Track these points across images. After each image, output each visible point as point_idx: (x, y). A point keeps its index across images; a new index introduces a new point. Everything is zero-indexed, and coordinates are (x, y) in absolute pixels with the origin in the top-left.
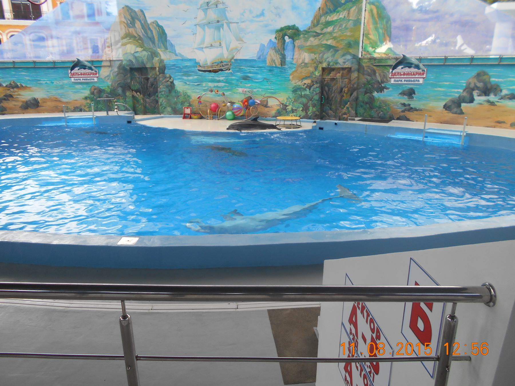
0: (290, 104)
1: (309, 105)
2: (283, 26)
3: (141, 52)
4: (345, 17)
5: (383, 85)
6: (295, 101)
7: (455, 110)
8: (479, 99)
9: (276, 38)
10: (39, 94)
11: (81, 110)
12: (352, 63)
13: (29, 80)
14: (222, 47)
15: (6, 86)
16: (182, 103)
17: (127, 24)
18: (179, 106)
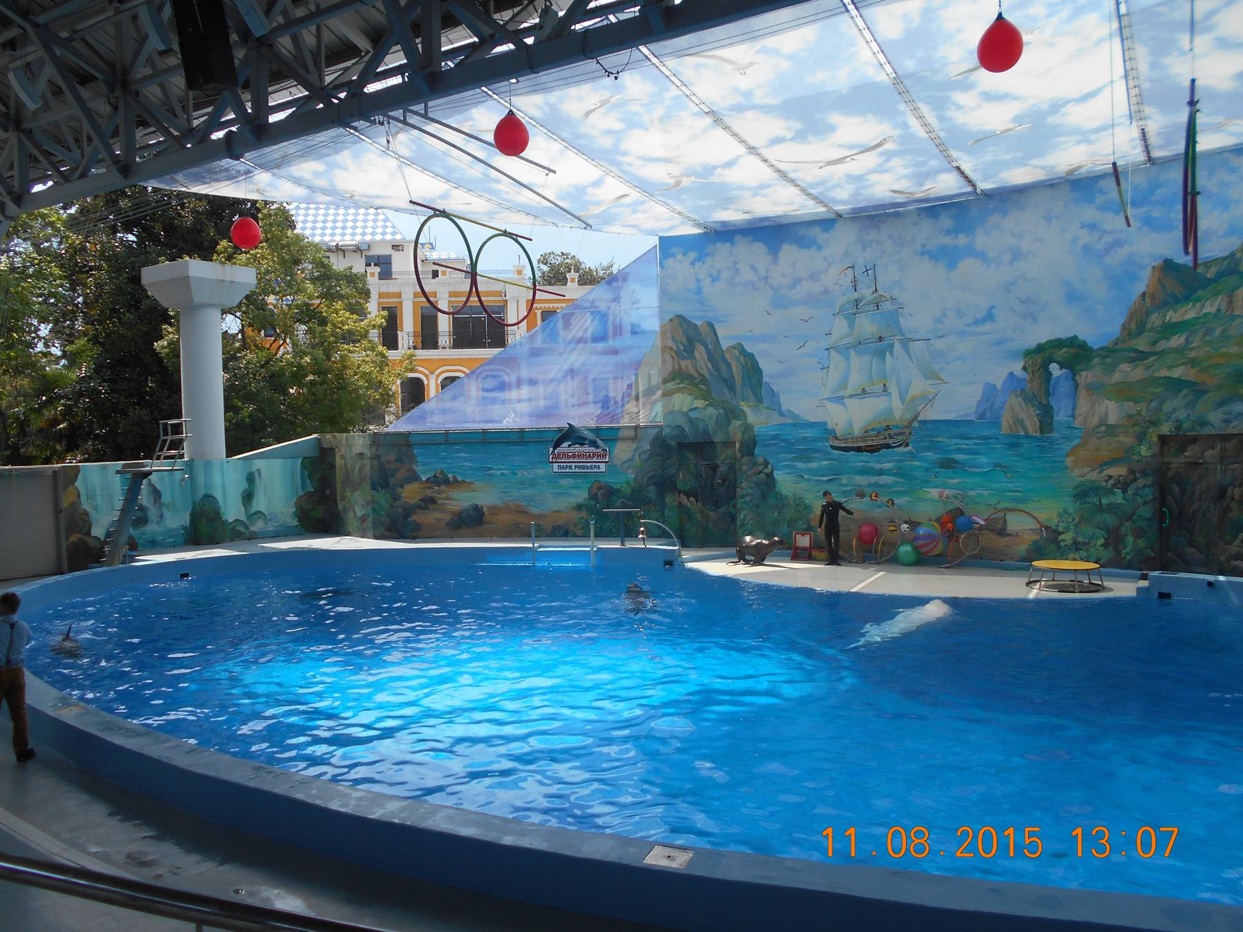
0: (1068, 529)
1: (1123, 528)
2: (1043, 341)
4: (1219, 310)
9: (1025, 368)
10: (485, 497)
13: (471, 469)
16: (792, 523)
17: (678, 353)
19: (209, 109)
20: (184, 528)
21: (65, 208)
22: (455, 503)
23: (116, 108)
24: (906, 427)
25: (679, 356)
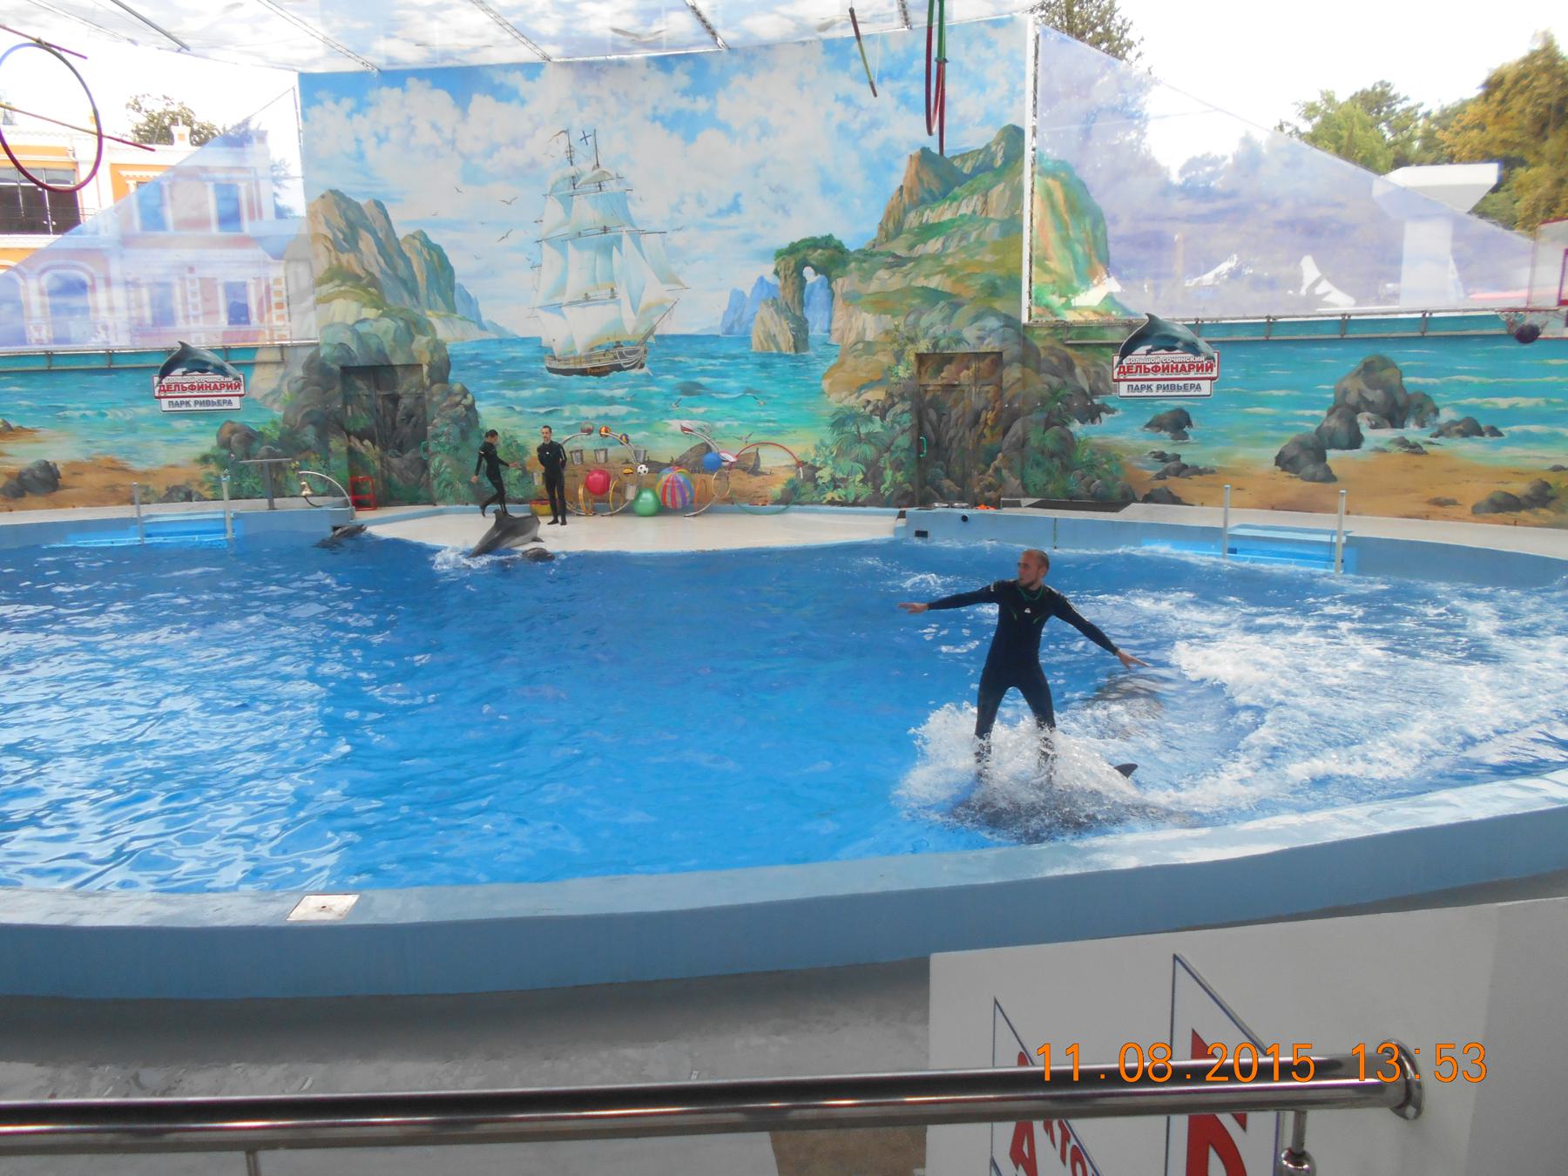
0: (825, 463)
1: (881, 463)
3: (376, 320)
4: (974, 212)
5: (1096, 401)
6: (841, 452)
7: (1310, 469)
8: (1376, 437)
9: (776, 273)
10: (59, 450)
11: (188, 497)
12: (1004, 340)
13: (32, 409)
14: (618, 303)
22: (9, 460)
25: (336, 246)
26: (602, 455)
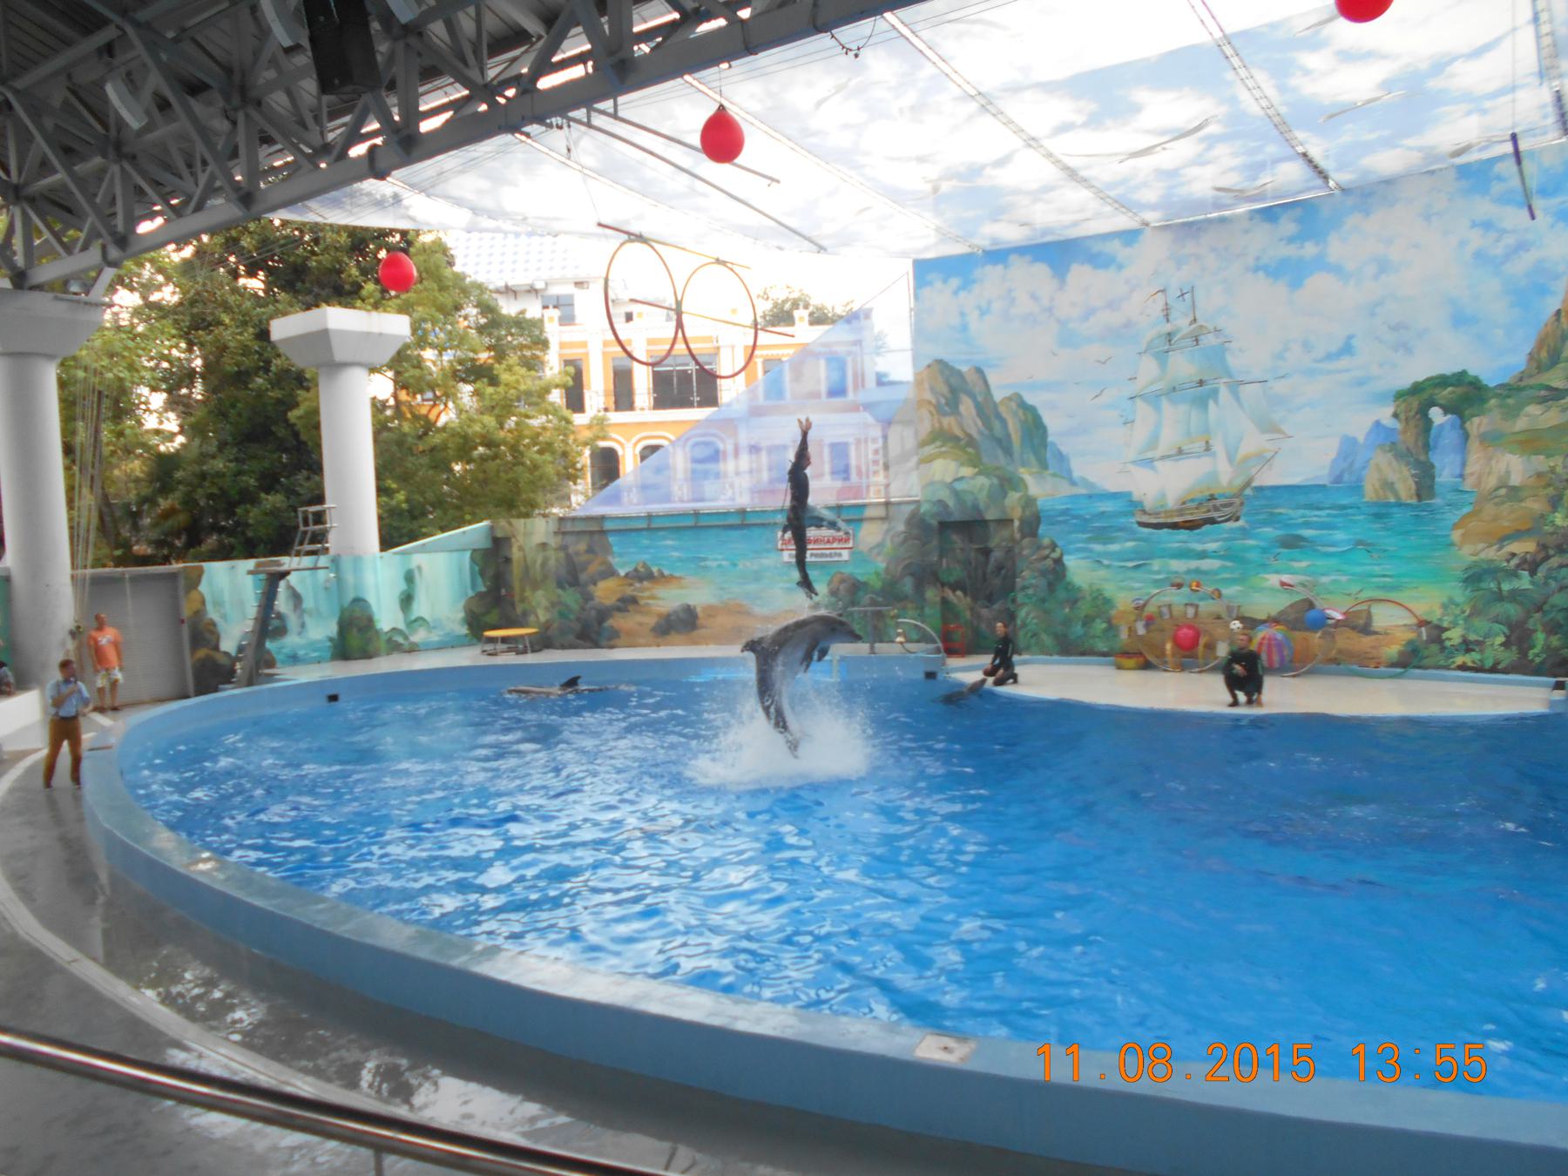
0: (1454, 624)
1: (1530, 624)
2: (1421, 378)
3: (972, 478)
9: (1395, 415)
10: (698, 595)
13: (680, 560)
14: (1214, 455)
15: (627, 575)
17: (938, 407)
18: (1078, 629)
19: (347, 119)
20: (331, 639)
21: (179, 250)
23: (234, 123)
24: (1235, 496)
25: (939, 410)
26: (1191, 612)
